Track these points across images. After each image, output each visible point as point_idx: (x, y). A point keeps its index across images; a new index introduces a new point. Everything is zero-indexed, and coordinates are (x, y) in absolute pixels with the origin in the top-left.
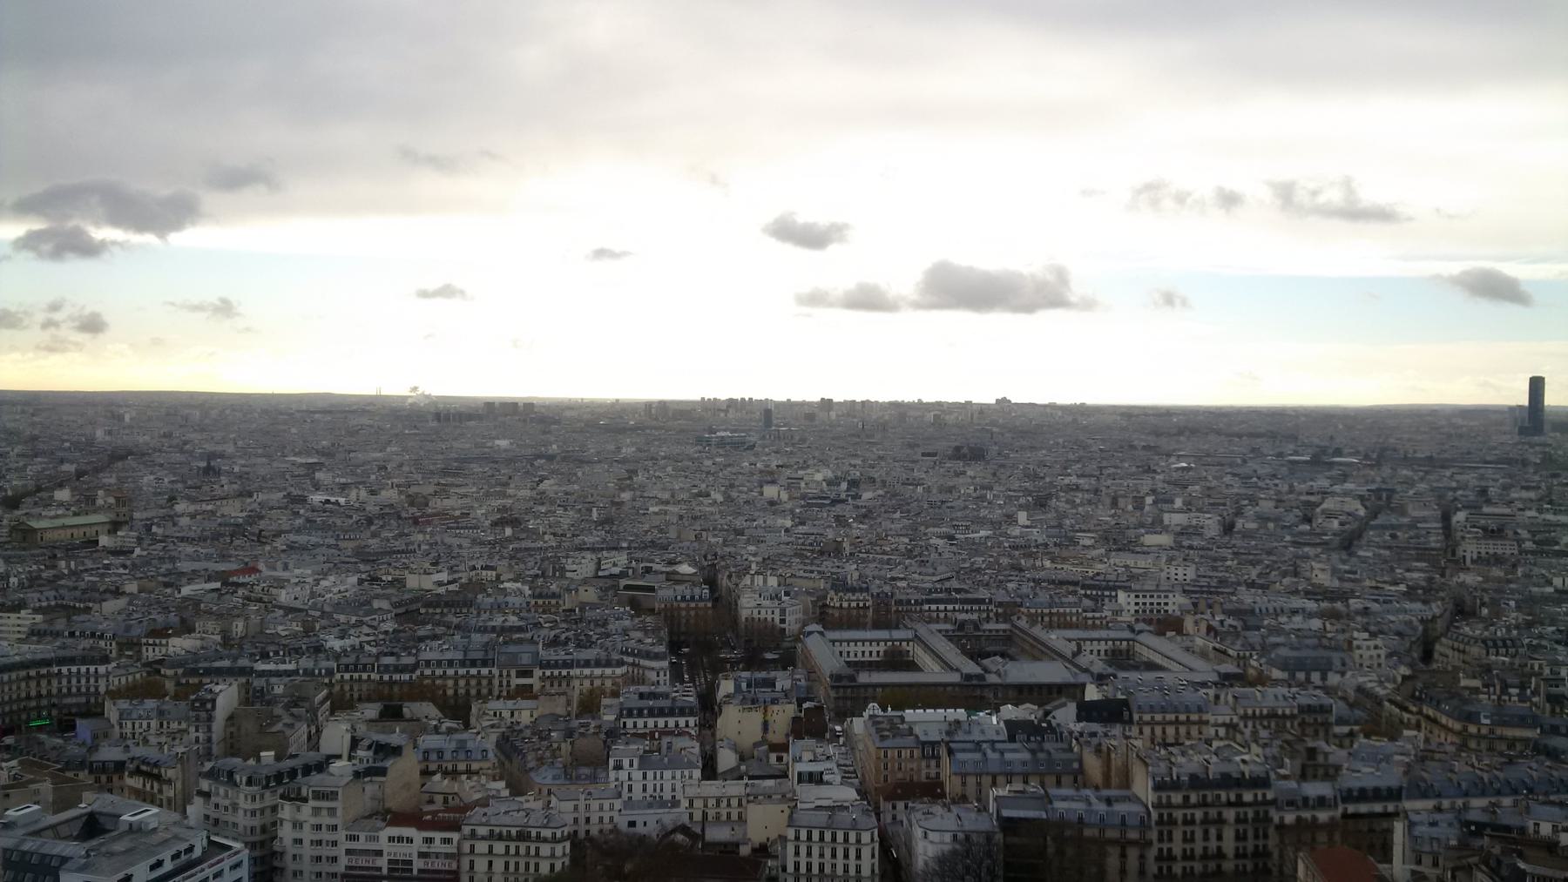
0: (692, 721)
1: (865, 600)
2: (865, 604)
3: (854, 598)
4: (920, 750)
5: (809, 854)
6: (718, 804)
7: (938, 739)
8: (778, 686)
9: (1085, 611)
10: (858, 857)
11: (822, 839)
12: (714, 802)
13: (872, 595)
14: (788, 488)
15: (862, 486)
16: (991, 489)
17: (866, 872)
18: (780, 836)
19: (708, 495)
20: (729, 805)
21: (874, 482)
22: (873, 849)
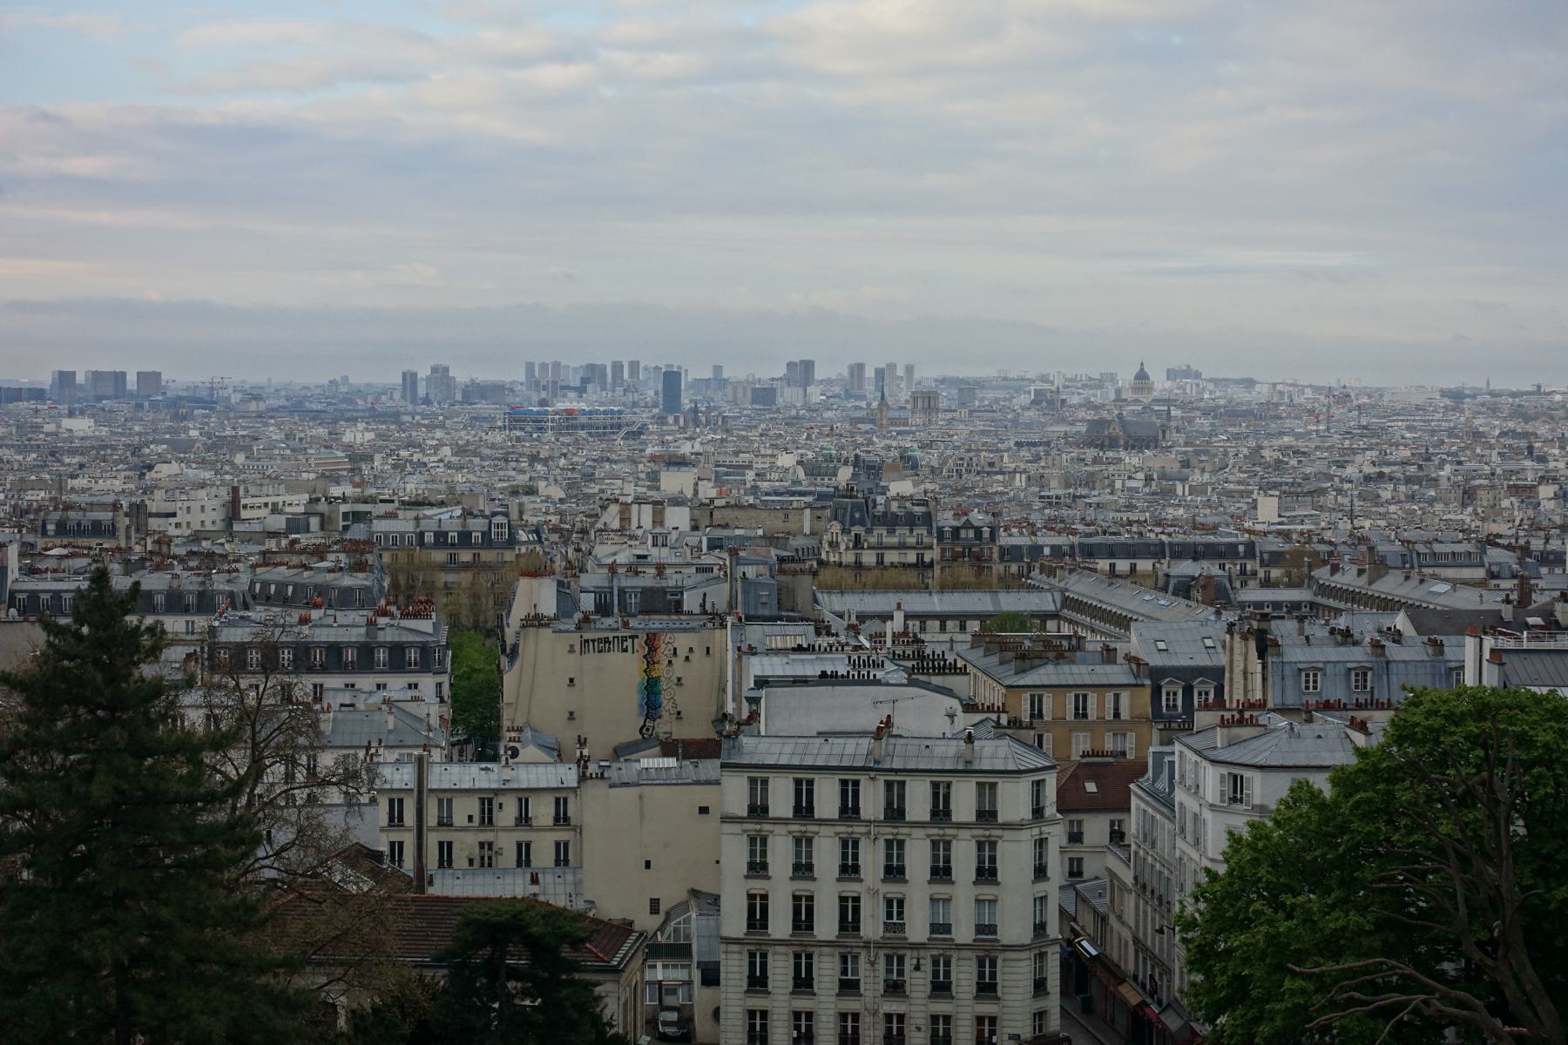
0: (427, 683)
1: (920, 546)
2: (920, 557)
3: (894, 540)
4: (1148, 691)
5: (803, 869)
6: (487, 819)
7: (1203, 660)
8: (691, 602)
9: (1492, 575)
10: (986, 873)
11: (849, 811)
12: (472, 806)
13: (940, 531)
14: (718, 481)
15: (885, 474)
16: (1184, 480)
17: (1014, 927)
18: (694, 893)
19: (531, 491)
20: (524, 820)
21: (915, 466)
22: (1041, 843)
